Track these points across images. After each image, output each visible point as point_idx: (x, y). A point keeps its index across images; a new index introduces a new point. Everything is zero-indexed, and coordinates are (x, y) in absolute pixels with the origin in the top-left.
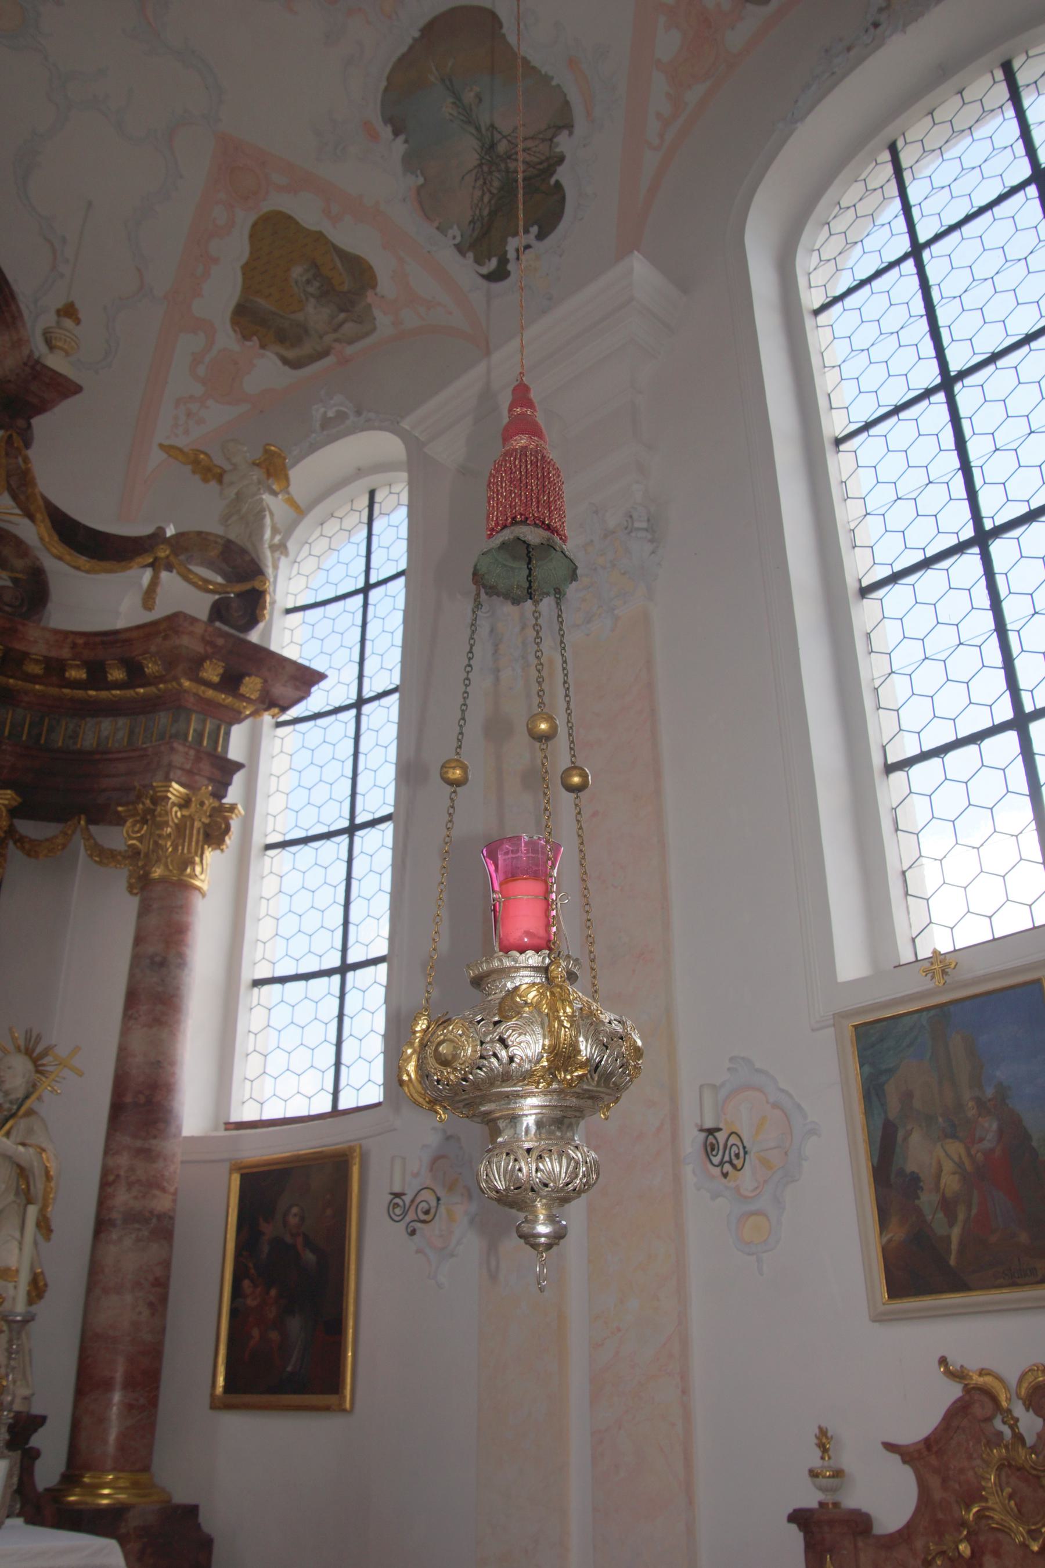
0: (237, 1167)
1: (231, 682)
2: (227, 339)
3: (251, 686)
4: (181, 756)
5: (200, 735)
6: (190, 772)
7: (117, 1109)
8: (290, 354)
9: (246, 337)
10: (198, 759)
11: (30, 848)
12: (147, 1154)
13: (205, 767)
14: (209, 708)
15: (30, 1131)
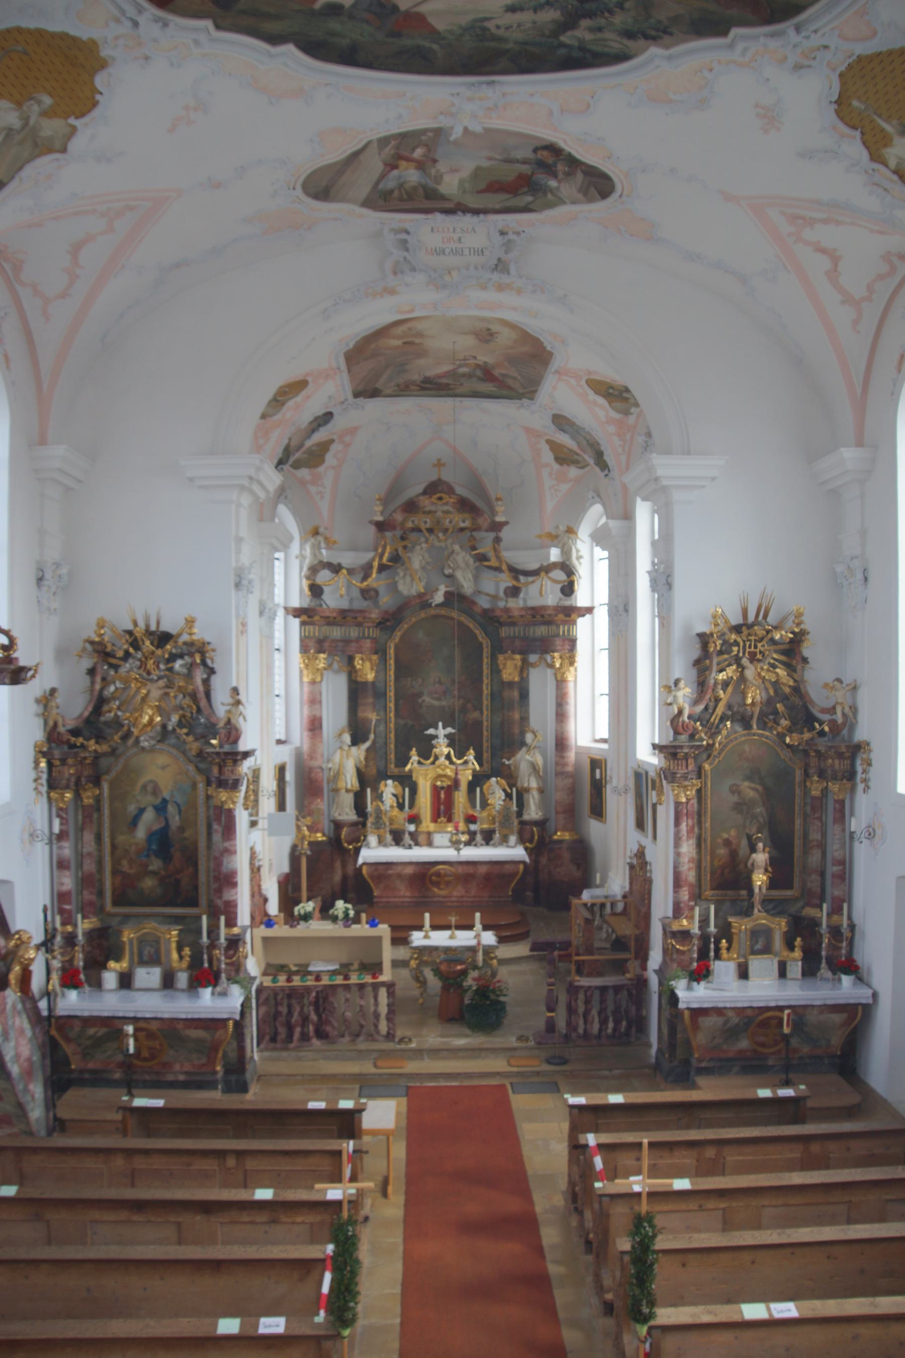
0: (589, 757)
1: (569, 615)
2: (556, 466)
3: (573, 616)
4: (558, 642)
5: (564, 632)
6: (562, 646)
7: (557, 745)
8: (579, 465)
9: (561, 464)
10: (564, 641)
11: (533, 665)
12: (562, 757)
13: (566, 642)
14: (565, 623)
15: (534, 754)
